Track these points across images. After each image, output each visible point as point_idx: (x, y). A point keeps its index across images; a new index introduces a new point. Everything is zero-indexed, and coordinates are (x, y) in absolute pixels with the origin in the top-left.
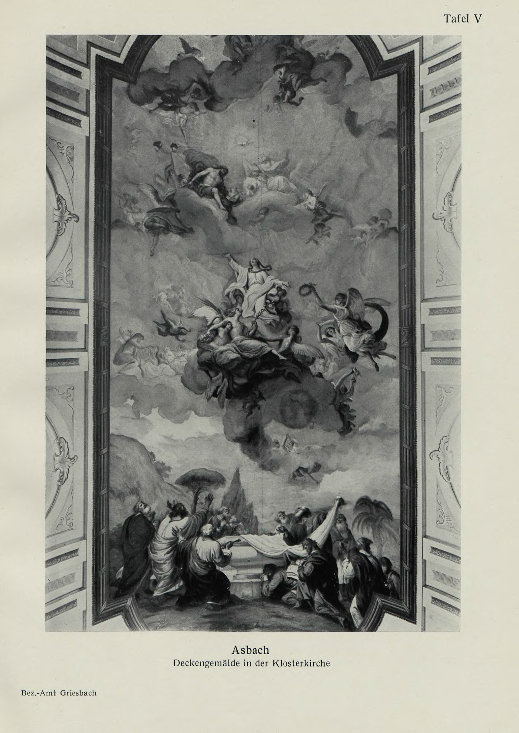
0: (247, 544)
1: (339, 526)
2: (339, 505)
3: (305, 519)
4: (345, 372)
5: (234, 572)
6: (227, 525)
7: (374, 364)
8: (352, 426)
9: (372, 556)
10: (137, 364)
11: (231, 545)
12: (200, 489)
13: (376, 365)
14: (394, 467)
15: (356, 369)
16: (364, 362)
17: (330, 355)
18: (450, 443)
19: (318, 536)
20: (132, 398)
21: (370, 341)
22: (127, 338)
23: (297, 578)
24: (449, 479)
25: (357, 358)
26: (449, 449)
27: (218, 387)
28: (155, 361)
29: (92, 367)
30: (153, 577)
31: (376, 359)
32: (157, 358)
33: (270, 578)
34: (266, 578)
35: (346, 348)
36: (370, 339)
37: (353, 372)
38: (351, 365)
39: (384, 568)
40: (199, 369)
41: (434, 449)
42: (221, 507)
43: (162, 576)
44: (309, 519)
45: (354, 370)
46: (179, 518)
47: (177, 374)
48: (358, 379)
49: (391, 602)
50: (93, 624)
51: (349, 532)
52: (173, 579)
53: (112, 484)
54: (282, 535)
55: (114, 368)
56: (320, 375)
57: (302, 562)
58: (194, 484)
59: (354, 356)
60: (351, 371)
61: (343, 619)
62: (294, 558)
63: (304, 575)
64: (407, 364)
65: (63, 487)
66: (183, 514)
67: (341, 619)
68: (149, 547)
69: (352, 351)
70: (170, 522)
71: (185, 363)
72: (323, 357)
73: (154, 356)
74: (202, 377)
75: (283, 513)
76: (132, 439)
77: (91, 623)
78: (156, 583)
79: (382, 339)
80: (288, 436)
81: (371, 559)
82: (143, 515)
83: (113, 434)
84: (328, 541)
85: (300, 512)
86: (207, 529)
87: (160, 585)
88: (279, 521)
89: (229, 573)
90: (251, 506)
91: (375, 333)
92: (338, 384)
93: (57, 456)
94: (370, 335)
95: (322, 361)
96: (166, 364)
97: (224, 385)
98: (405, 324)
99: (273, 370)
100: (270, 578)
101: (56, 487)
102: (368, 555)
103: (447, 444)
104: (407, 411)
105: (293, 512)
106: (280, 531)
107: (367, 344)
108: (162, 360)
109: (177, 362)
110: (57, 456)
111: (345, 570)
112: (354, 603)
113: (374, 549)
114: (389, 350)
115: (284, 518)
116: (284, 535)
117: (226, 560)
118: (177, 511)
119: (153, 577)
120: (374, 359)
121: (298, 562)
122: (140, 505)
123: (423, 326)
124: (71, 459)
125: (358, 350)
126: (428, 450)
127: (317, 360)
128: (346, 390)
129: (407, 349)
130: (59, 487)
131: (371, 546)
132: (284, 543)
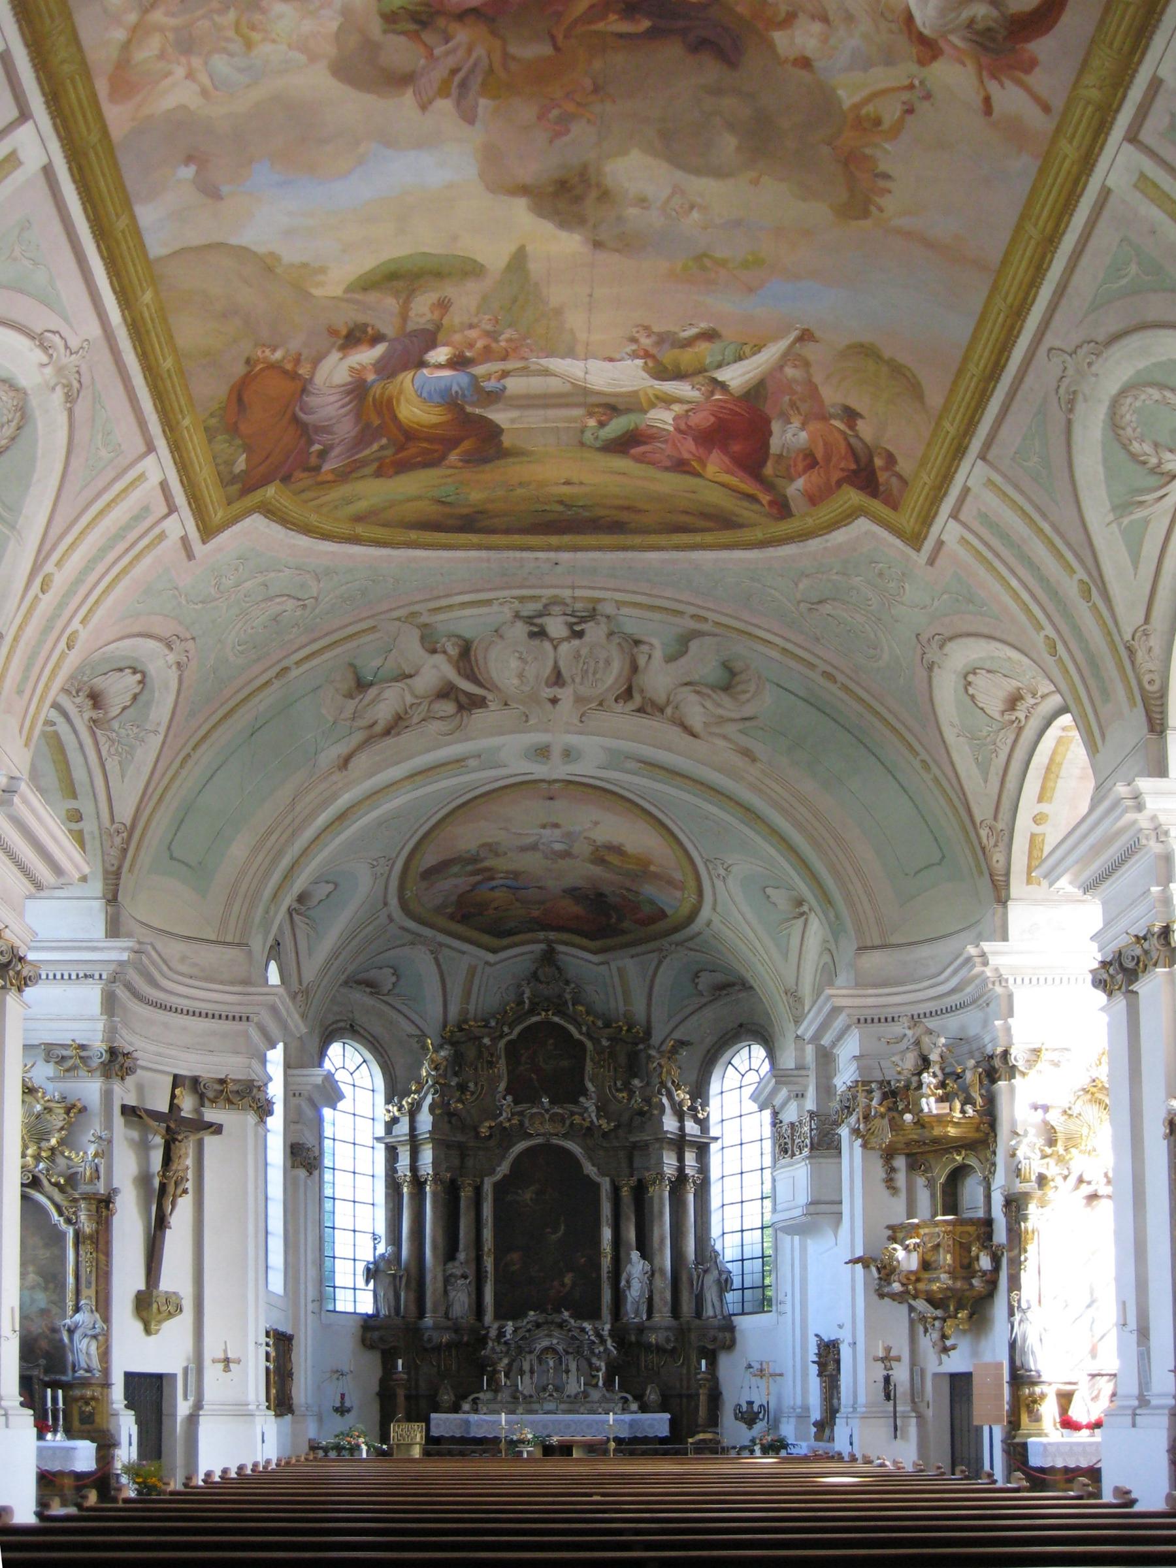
0: (546, 373)
1: (790, 372)
2: (801, 339)
3: (703, 347)
4: (882, 77)
5: (514, 414)
6: (494, 345)
7: (982, 94)
8: (873, 208)
9: (857, 436)
10: (180, 72)
11: (505, 374)
12: (414, 290)
13: (987, 100)
14: (957, 328)
15: (921, 83)
16: (954, 76)
17: (849, 18)
18: (1100, 360)
19: (736, 376)
20: (189, 159)
21: (989, 29)
22: (132, 18)
23: (672, 429)
24: (1071, 410)
25: (934, 58)
26: (1094, 369)
27: (454, 72)
28: (237, 46)
29: (55, 146)
30: (317, 447)
31: (993, 87)
32: (242, 36)
33: (602, 424)
34: (592, 423)
35: (910, 18)
36: (992, 24)
37: (911, 87)
38: (914, 68)
39: (878, 462)
40: (385, 32)
41: (1063, 347)
42: (477, 315)
43: (337, 441)
44: (716, 346)
45: (917, 83)
46: (363, 348)
47: (313, 58)
48: (923, 107)
49: (876, 505)
50: (204, 542)
51: (813, 391)
52: (366, 435)
53: (180, 342)
54: (640, 362)
55: (118, 117)
56: (805, 63)
57: (686, 407)
58: (400, 284)
59: (928, 48)
60: (907, 82)
61: (768, 498)
62: (667, 401)
63: (689, 426)
64: (1075, 143)
65: (78, 409)
66: (376, 339)
67: (765, 498)
68: (297, 409)
69: (926, 32)
70: (341, 359)
71: (334, 26)
72: (825, 19)
73: (231, 33)
74: (400, 51)
75: (647, 328)
76: (210, 246)
77: (200, 542)
78: (323, 454)
79: (1028, 39)
80: (677, 190)
81: (853, 440)
82: (273, 367)
83: (160, 259)
84: (756, 392)
85: (693, 331)
86: (440, 355)
87: (334, 454)
88: (634, 340)
89: (499, 416)
90: (558, 312)
91: (1012, 15)
92: (857, 99)
93: (44, 365)
94: (995, 13)
95: (817, 27)
96: (274, 41)
97: (475, 65)
98: (1111, 44)
99: (646, 24)
100: (602, 424)
101: (65, 415)
102: (849, 432)
103: (1094, 357)
104: (1033, 242)
105: (676, 329)
106: (634, 355)
107: (977, 33)
108: (256, 36)
109: (307, 26)
110: (44, 365)
111: (789, 436)
112: (800, 483)
113: (865, 429)
114: (1038, 79)
115: (648, 336)
116: (646, 363)
117: (494, 397)
118: (354, 337)
119: (317, 447)
120: (986, 80)
121: (677, 408)
122: (259, 353)
123: (1156, 85)
124: (77, 353)
125: (944, 36)
126: (1049, 340)
127: (802, 20)
128: (878, 122)
129: (1090, 109)
130: (70, 412)
131: (860, 422)
132: (646, 375)
